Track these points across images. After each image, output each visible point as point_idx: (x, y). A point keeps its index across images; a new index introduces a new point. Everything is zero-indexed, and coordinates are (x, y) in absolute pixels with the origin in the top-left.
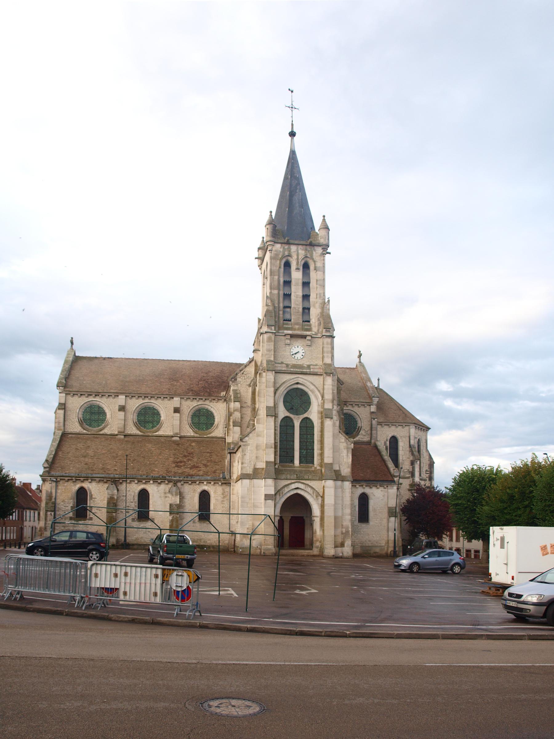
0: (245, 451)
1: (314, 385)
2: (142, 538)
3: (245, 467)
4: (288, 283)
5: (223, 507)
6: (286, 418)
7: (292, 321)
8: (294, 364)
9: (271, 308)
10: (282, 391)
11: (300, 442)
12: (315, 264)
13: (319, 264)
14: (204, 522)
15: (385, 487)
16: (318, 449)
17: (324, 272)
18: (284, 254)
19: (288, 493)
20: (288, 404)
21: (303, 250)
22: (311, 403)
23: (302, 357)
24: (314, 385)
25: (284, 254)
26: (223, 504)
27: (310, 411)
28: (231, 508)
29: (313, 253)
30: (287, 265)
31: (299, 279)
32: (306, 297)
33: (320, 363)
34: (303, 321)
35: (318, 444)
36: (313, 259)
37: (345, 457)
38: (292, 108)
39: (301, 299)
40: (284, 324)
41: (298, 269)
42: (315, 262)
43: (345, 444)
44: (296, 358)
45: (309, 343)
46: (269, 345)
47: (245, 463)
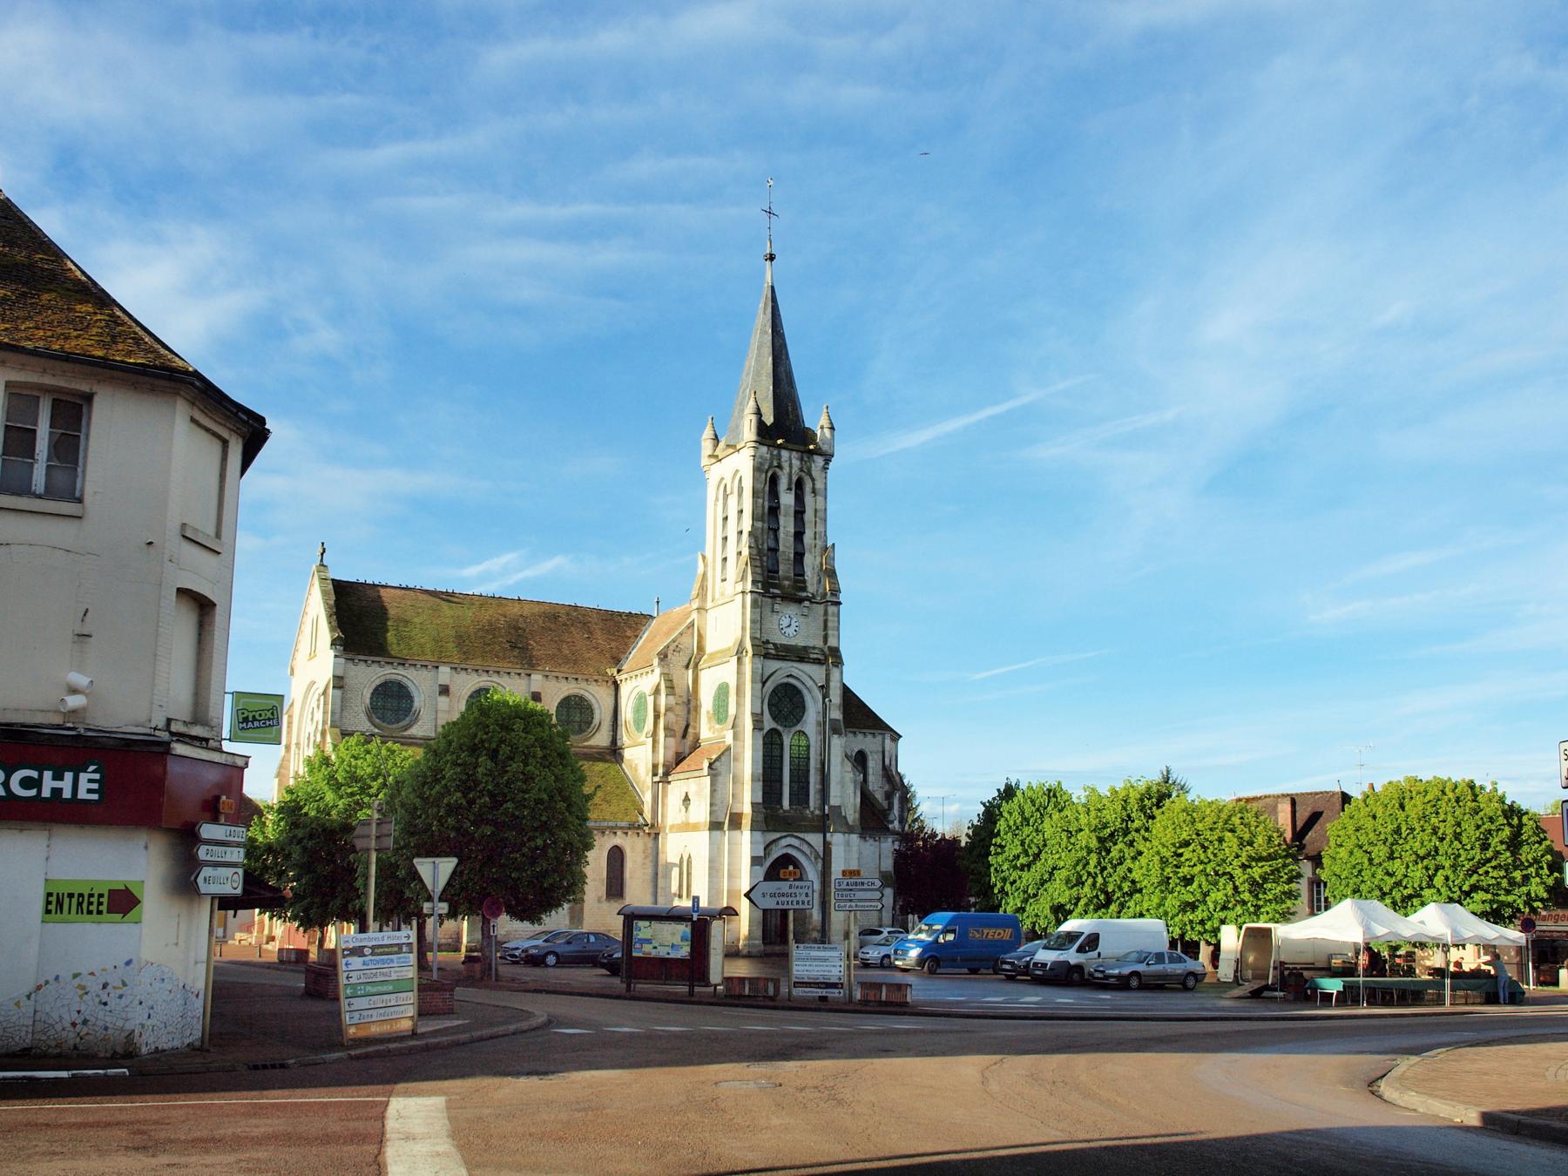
0: (715, 784)
1: (814, 681)
2: (516, 931)
3: (715, 811)
4: (774, 511)
5: (644, 874)
6: (773, 731)
7: (781, 572)
8: (784, 645)
9: (755, 552)
10: (770, 686)
11: (791, 770)
12: (814, 484)
13: (819, 485)
14: (616, 901)
15: (877, 838)
16: (815, 784)
17: (826, 498)
18: (772, 463)
19: (776, 853)
20: (774, 709)
21: (797, 459)
22: (807, 709)
23: (795, 633)
24: (814, 681)
25: (772, 463)
26: (644, 869)
27: (805, 721)
28: (660, 875)
29: (811, 467)
30: (774, 481)
31: (790, 506)
32: (799, 535)
33: (820, 643)
34: (795, 575)
35: (816, 773)
36: (811, 476)
37: (852, 795)
38: (770, 213)
39: (792, 539)
40: (769, 577)
41: (789, 489)
42: (813, 480)
43: (851, 775)
44: (787, 635)
45: (805, 610)
46: (754, 613)
47: (716, 805)
